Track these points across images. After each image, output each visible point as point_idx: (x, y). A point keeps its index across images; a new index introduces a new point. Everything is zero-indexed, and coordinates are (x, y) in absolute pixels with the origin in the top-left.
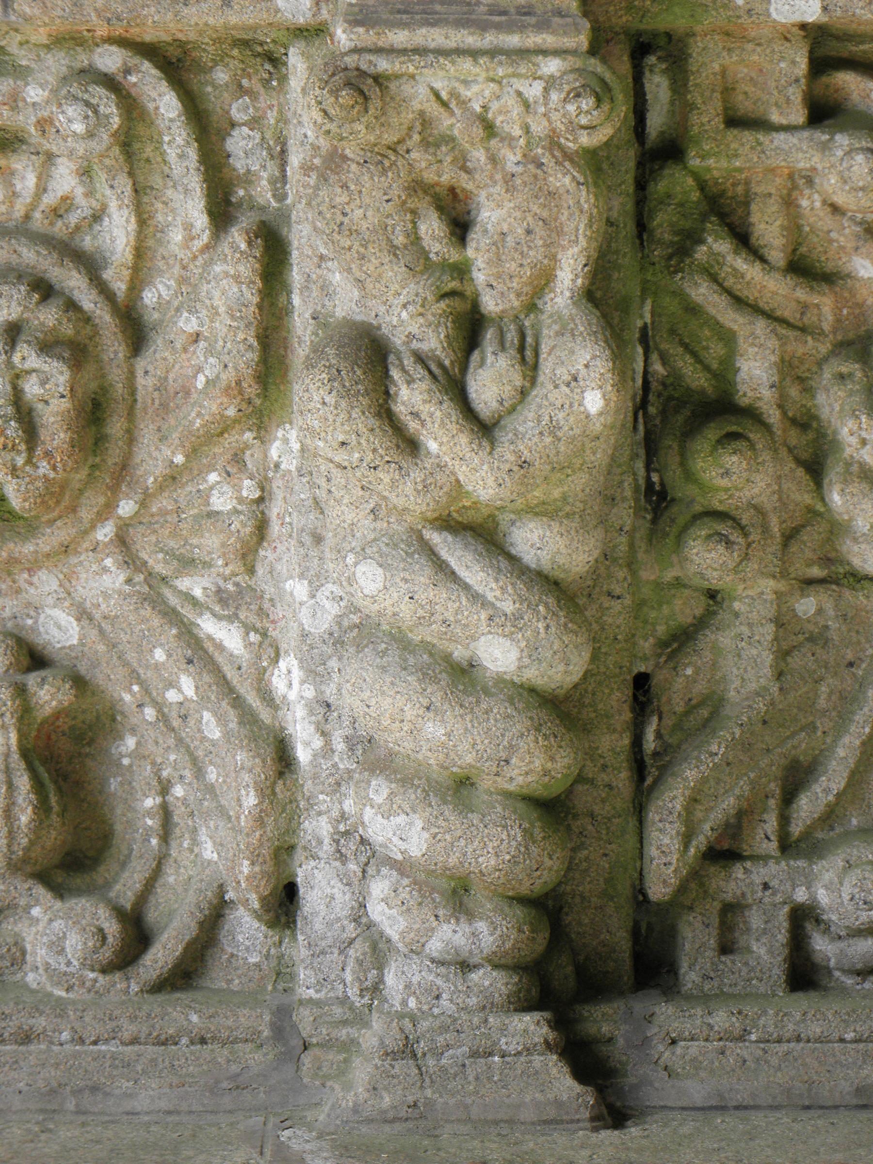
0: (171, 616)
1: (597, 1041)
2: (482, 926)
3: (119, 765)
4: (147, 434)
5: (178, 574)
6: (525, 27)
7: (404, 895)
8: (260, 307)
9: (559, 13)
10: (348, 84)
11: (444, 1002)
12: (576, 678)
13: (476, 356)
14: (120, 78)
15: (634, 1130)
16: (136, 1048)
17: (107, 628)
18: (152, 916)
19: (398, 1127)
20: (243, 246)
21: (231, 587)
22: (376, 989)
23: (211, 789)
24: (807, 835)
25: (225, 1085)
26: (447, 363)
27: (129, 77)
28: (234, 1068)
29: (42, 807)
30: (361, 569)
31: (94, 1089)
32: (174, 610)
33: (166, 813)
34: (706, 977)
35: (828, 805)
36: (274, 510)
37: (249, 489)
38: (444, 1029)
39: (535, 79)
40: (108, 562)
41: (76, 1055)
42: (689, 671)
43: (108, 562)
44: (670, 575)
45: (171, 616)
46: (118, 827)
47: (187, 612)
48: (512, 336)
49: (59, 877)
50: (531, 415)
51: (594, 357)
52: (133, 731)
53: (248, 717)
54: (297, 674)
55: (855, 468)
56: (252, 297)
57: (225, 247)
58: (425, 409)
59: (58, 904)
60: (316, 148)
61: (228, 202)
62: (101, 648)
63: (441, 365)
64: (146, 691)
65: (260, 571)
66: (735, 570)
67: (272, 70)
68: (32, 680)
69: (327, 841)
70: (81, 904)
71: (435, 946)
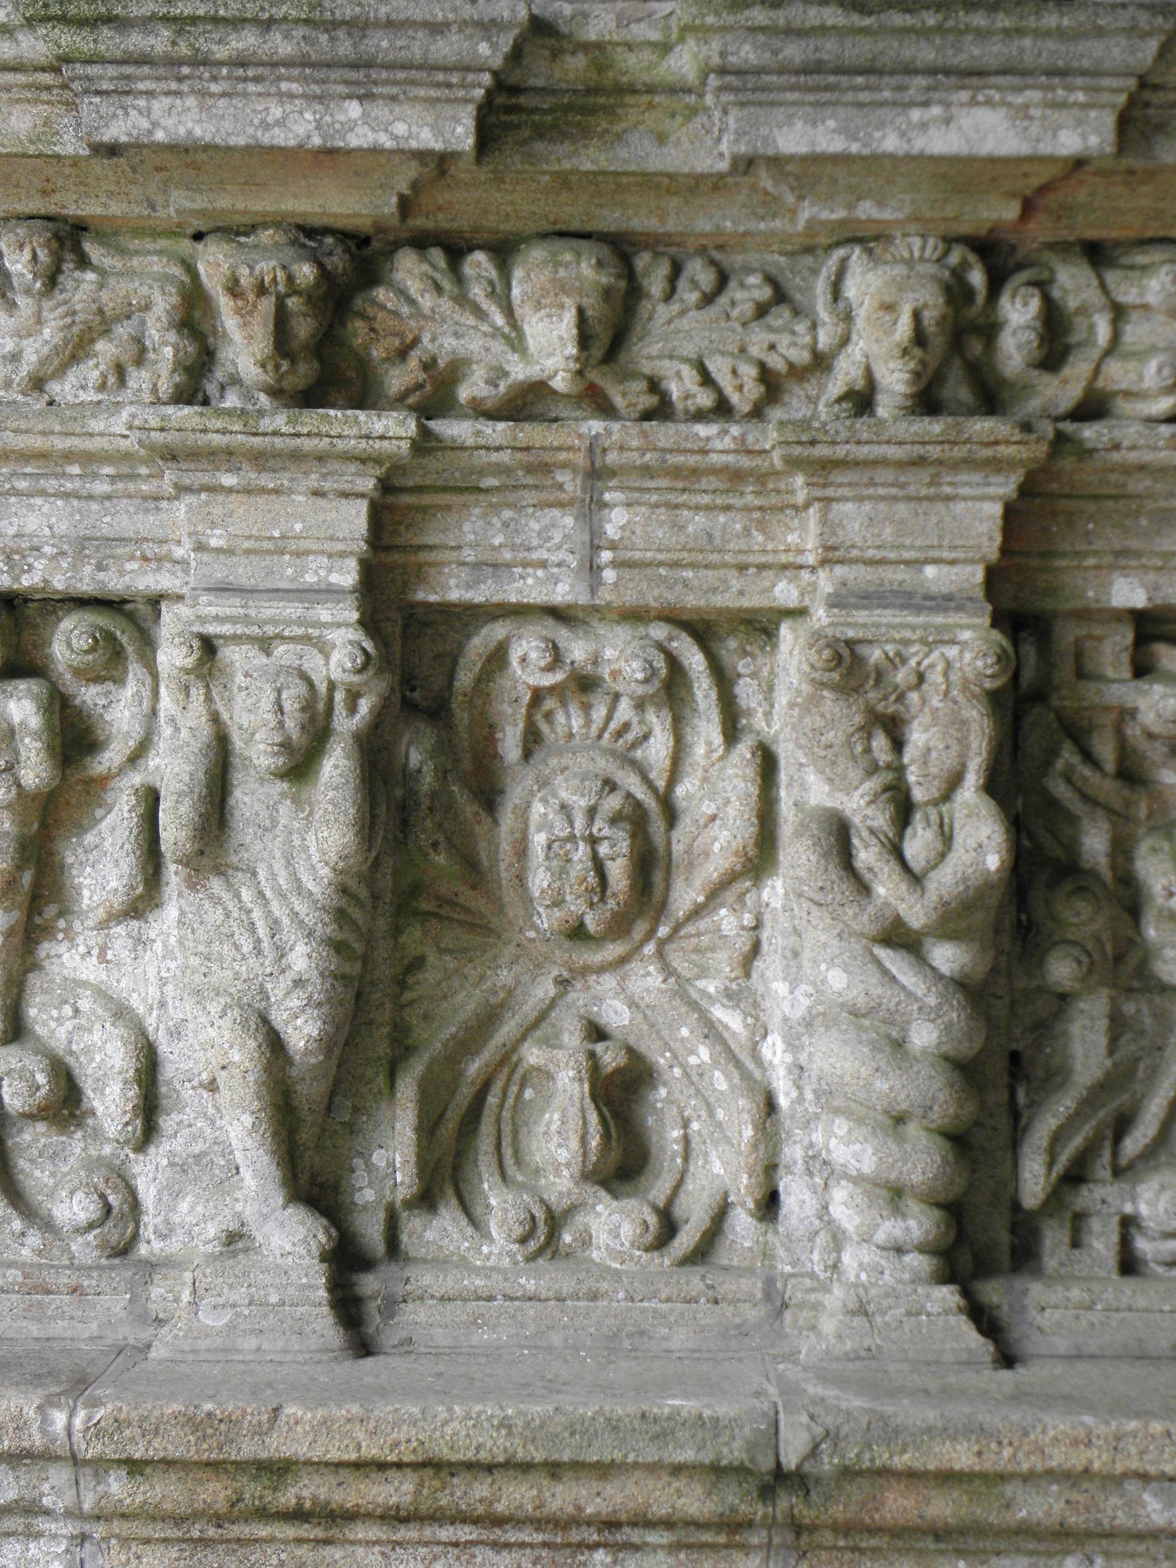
0: (694, 1006)
1: (991, 1308)
2: (912, 1223)
3: (655, 1108)
4: (678, 884)
5: (698, 977)
7: (858, 1200)
8: (759, 796)
9: (970, 599)
10: (828, 646)
11: (887, 1276)
12: (974, 1052)
13: (909, 831)
14: (665, 644)
15: (1021, 1372)
16: (670, 1305)
17: (649, 1013)
18: (678, 1212)
19: (858, 1364)
20: (749, 756)
21: (734, 986)
22: (835, 1267)
23: (719, 1125)
24: (1131, 1166)
25: (732, 1332)
26: (891, 835)
28: (737, 1320)
29: (606, 1136)
30: (831, 974)
31: (642, 1333)
33: (686, 1140)
34: (1062, 1264)
35: (1147, 1146)
36: (765, 935)
37: (748, 919)
38: (887, 1295)
40: (651, 968)
41: (629, 1310)
42: (1048, 1050)
43: (651, 968)
44: (1034, 983)
45: (694, 1006)
46: (654, 1150)
47: (704, 1003)
48: (934, 817)
49: (615, 1185)
50: (949, 871)
52: (665, 1084)
53: (746, 1075)
54: (780, 1046)
56: (754, 790)
58: (877, 866)
59: (615, 1203)
60: (798, 691)
61: (735, 728)
62: (645, 1027)
63: (887, 837)
64: (675, 1056)
65: (755, 975)
66: (1083, 980)
68: (599, 1048)
69: (800, 1162)
70: (631, 1203)
71: (880, 1236)
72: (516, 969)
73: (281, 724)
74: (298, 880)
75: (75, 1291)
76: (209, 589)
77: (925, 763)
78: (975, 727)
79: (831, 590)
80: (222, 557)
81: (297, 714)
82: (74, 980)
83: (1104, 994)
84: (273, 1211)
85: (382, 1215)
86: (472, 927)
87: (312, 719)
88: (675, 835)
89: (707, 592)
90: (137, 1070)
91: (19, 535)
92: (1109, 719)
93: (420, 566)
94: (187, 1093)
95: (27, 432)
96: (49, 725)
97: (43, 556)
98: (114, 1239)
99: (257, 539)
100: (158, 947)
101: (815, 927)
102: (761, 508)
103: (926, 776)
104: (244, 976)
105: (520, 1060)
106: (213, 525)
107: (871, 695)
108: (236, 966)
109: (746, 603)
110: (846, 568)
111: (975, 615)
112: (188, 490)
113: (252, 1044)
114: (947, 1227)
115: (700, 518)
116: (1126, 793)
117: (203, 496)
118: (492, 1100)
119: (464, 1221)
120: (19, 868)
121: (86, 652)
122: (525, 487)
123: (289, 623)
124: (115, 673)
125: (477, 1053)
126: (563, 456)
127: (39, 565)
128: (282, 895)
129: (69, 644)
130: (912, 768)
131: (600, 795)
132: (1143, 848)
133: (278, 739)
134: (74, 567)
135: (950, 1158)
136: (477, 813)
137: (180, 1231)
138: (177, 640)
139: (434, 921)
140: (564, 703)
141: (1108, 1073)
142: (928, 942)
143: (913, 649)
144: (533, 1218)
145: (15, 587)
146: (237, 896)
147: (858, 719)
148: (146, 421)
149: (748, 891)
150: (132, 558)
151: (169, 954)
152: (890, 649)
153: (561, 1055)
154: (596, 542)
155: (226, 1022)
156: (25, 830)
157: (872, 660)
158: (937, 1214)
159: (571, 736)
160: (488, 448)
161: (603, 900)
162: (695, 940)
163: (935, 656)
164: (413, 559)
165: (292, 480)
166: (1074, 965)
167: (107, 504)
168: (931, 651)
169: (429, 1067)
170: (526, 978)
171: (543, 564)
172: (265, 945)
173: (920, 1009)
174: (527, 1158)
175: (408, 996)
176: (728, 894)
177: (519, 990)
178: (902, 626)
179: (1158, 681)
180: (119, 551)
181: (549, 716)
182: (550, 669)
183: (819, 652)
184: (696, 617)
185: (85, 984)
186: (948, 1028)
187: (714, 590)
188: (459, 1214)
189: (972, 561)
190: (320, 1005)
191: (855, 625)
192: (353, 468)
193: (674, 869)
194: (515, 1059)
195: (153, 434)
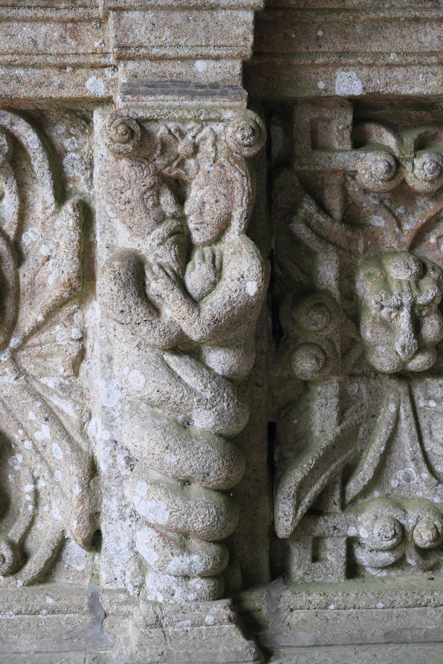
0: (37, 396)
1: (254, 611)
5: (42, 376)
6: (214, 95)
8: (79, 241)
9: (231, 87)
10: (123, 123)
12: (241, 429)
13: (190, 266)
14: (8, 127)
16: (20, 616)
17: (6, 402)
18: (30, 545)
21: (67, 382)
22: (141, 586)
23: (58, 484)
24: (354, 501)
26: (175, 269)
27: (13, 127)
32: (39, 394)
33: (36, 493)
35: (364, 486)
37: (75, 333)
38: (177, 611)
39: (220, 121)
42: (295, 422)
43: (7, 370)
45: (37, 396)
46: (13, 501)
48: (208, 255)
50: (219, 296)
51: (251, 265)
53: (76, 448)
55: (378, 320)
56: (75, 236)
57: (63, 212)
58: (164, 293)
63: (173, 271)
64: (26, 434)
65: (81, 374)
66: (320, 371)
67: (85, 124)
77: (201, 213)
78: (238, 184)
79: (125, 81)
83: (335, 380)
88: (22, 271)
89: (35, 86)
92: (336, 180)
101: (120, 341)
102: (72, 21)
103: (202, 223)
107: (158, 162)
109: (65, 94)
110: (136, 64)
111: (236, 99)
114: (222, 558)
115: (27, 29)
116: (349, 233)
130: (191, 218)
132: (361, 275)
135: (223, 509)
141: (337, 437)
142: (205, 349)
143: (189, 126)
147: (149, 181)
149: (75, 312)
152: (172, 126)
157: (158, 135)
158: (213, 549)
162: (38, 348)
163: (206, 130)
166: (314, 362)
168: (202, 127)
173: (199, 401)
176: (60, 314)
178: (180, 107)
179: (372, 150)
183: (116, 128)
184: (31, 108)
186: (220, 415)
187: (40, 85)
189: (232, 58)
191: (144, 108)
193: (21, 296)
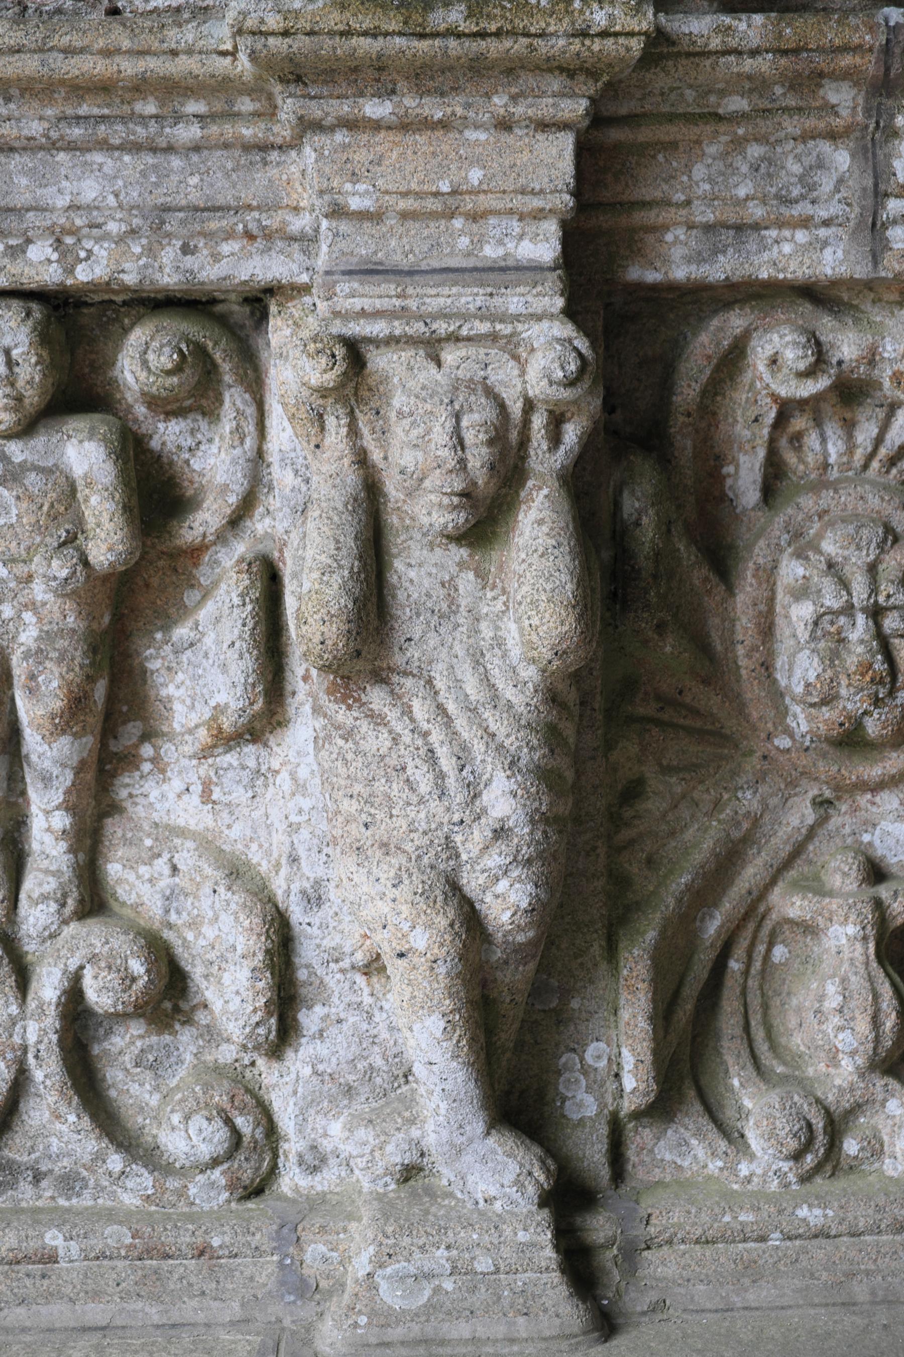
68: (884, 892)
72: (763, 789)
73: (462, 463)
74: (492, 687)
75: (201, 1254)
76: (350, 273)
80: (367, 225)
81: (485, 450)
82: (167, 826)
84: (471, 1141)
85: (604, 1130)
86: (701, 735)
87: (503, 455)
90: (267, 951)
91: (74, 207)
93: (633, 230)
94: (333, 980)
95: (82, 51)
96: (124, 476)
97: (106, 236)
98: (247, 1175)
99: (418, 195)
100: (284, 779)
104: (424, 826)
105: (769, 910)
106: (354, 177)
108: (411, 812)
112: (317, 126)
113: (442, 922)
117: (340, 137)
118: (734, 965)
119: (713, 1133)
120: (90, 679)
121: (169, 373)
122: (785, 110)
123: (466, 317)
124: (204, 402)
125: (716, 905)
126: (846, 60)
127: (101, 252)
128: (473, 710)
129: (145, 363)
131: (881, 546)
133: (458, 485)
134: (150, 251)
136: (706, 580)
137: (332, 1161)
138: (312, 347)
139: (655, 731)
140: (818, 422)
144: (809, 1125)
145: (69, 282)
146: (407, 712)
148: (262, 21)
150: (229, 235)
151: (300, 788)
153: (834, 904)
154: (882, 187)
155: (405, 892)
156: (95, 626)
159: (826, 466)
160: (738, 52)
161: (892, 693)
164: (624, 221)
165: (468, 106)
167: (195, 158)
169: (663, 933)
170: (774, 801)
171: (805, 223)
172: (451, 782)
174: (783, 1041)
175: (626, 834)
177: (767, 818)
180: (213, 225)
181: (797, 439)
182: (809, 373)
185: (183, 832)
188: (704, 1121)
190: (529, 862)
192: (556, 83)
194: (762, 909)
195: (271, 41)
